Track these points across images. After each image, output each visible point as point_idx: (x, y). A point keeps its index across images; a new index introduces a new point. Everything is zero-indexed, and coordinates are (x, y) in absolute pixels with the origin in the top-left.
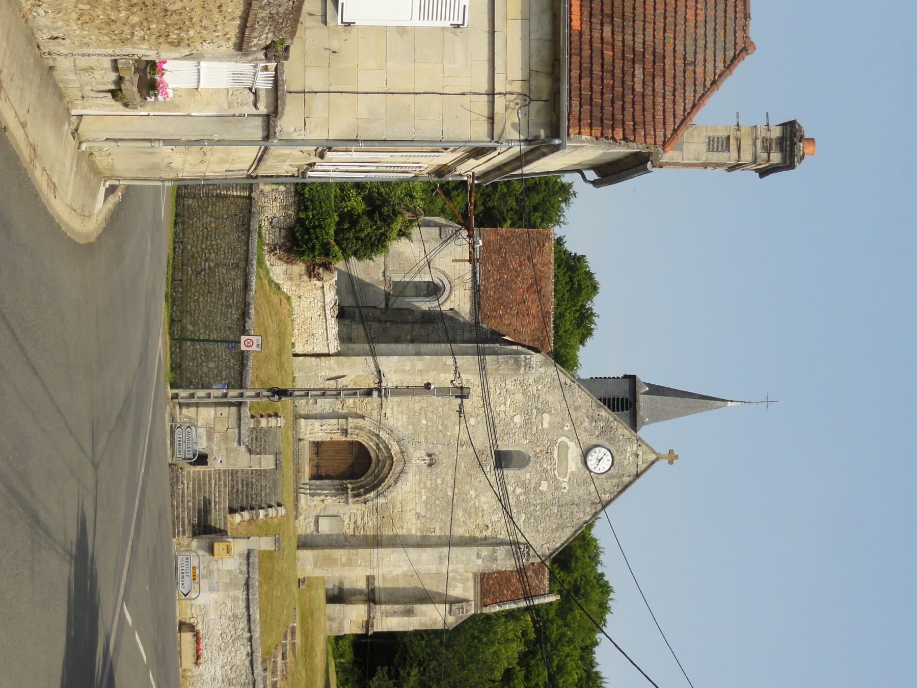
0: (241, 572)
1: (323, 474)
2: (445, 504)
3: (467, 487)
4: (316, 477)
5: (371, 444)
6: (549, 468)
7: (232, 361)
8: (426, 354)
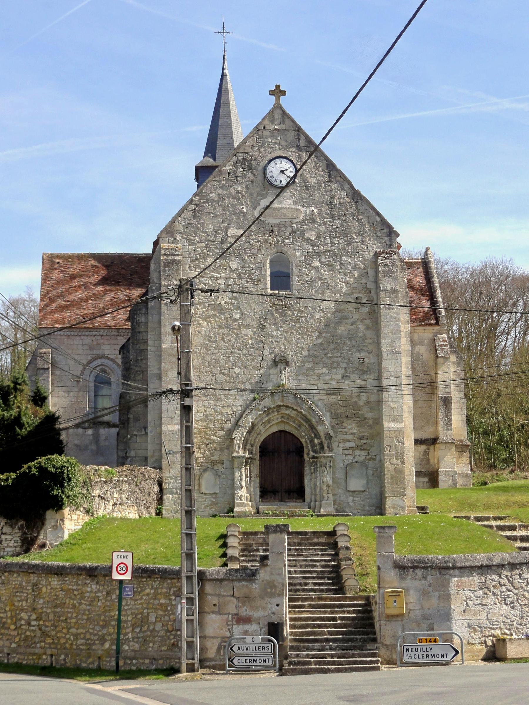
0: (424, 578)
2: (332, 346)
3: (312, 321)
6: (289, 229)
7: (148, 591)
8: (160, 369)
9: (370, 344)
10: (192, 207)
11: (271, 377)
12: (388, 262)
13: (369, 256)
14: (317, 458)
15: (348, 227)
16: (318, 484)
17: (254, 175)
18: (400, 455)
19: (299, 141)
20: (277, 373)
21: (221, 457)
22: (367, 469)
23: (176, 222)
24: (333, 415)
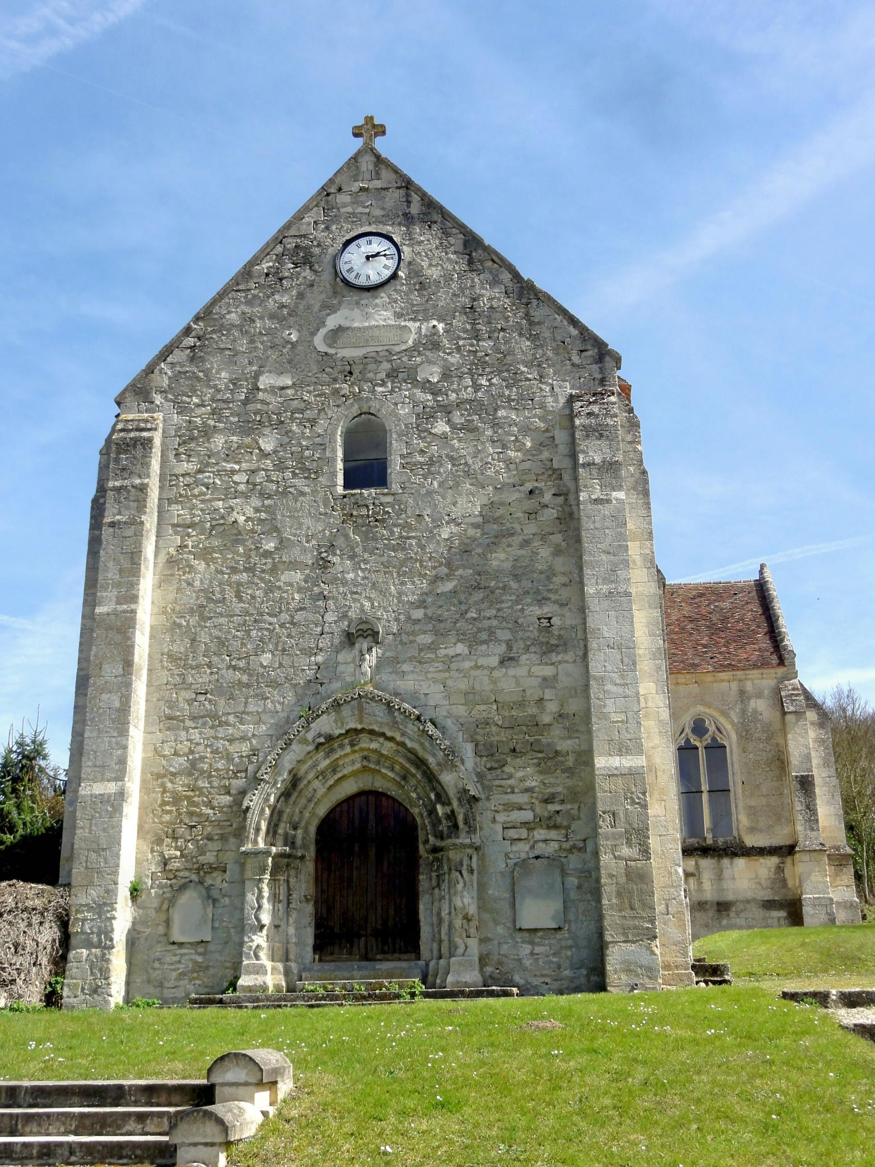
2: (478, 595)
6: (386, 366)
9: (564, 585)
10: (190, 341)
11: (341, 668)
12: (595, 409)
13: (556, 403)
14: (441, 849)
15: (510, 352)
16: (444, 914)
17: (316, 272)
18: (638, 835)
19: (409, 207)
20: (353, 661)
21: (221, 854)
22: (564, 873)
23: (156, 371)
24: (481, 747)
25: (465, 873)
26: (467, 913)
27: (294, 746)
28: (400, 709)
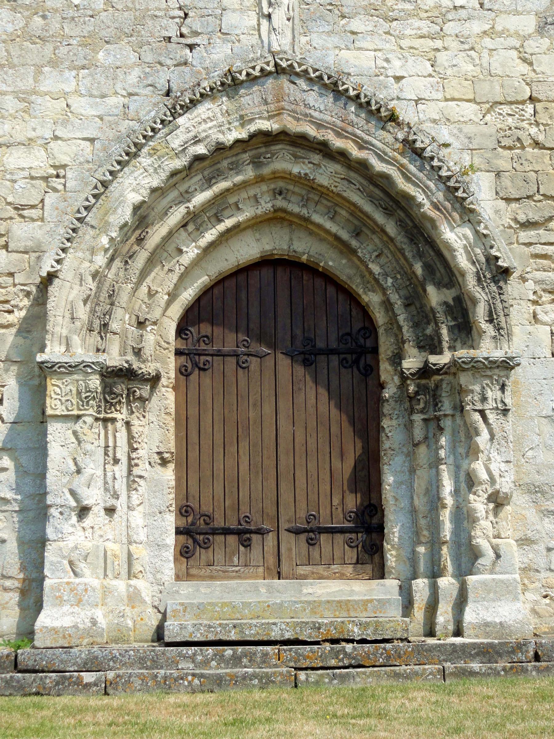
1: (352, 502)
4: (365, 538)
5: (191, 252)
24: (506, 181)
25: (491, 417)
26: (498, 492)
27: (144, 160)
28: (358, 96)
